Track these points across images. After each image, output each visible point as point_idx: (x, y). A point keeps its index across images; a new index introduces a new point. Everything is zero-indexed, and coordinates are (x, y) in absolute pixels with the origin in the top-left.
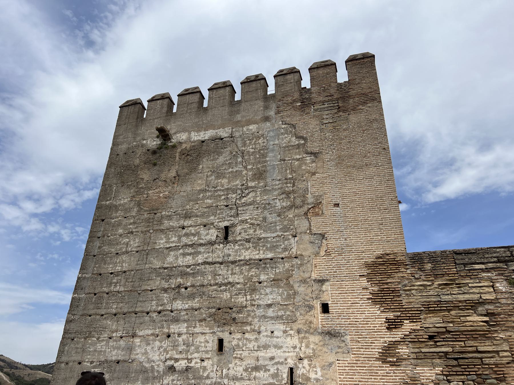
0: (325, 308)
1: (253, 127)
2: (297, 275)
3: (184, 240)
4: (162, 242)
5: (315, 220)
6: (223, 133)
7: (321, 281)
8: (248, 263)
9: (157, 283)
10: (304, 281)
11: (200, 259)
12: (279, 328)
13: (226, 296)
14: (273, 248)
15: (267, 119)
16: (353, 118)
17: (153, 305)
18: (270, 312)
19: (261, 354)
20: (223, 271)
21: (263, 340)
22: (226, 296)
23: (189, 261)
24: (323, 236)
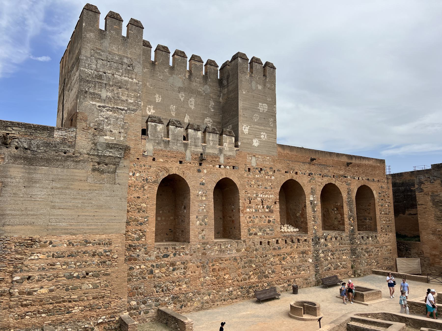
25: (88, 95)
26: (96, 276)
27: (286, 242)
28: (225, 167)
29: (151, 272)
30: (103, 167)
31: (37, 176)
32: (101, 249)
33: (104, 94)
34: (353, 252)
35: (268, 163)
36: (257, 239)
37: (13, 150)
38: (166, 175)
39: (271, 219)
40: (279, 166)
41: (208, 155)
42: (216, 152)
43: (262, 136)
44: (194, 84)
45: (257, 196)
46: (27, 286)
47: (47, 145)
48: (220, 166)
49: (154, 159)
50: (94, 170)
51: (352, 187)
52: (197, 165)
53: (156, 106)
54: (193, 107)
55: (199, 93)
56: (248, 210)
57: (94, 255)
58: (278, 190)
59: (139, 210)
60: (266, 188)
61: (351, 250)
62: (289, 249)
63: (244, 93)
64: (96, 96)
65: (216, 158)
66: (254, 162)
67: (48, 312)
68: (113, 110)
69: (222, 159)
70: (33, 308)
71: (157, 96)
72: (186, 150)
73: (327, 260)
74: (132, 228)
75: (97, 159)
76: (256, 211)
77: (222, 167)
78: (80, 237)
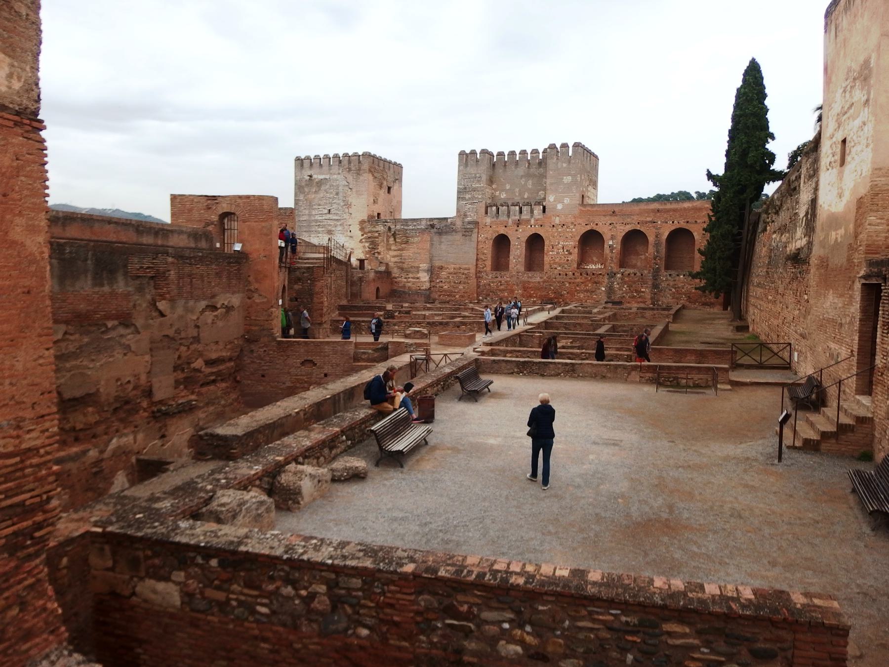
2: (345, 224)
3: (320, 212)
4: (314, 213)
6: (327, 177)
8: (335, 220)
9: (314, 224)
15: (339, 174)
16: (361, 178)
20: (329, 221)
23: (321, 218)
26: (464, 283)
27: (581, 274)
29: (489, 285)
30: (467, 233)
31: (443, 240)
32: (466, 272)
33: (468, 196)
34: (655, 286)
36: (556, 272)
37: (435, 230)
40: (580, 221)
41: (523, 220)
42: (528, 217)
43: (565, 201)
44: (532, 170)
45: (559, 243)
46: (441, 284)
51: (661, 231)
52: (516, 227)
53: (507, 191)
54: (530, 187)
55: (535, 176)
58: (578, 238)
59: (484, 254)
61: (653, 284)
64: (464, 199)
66: (557, 220)
67: (448, 295)
68: (471, 204)
74: (480, 263)
78: (458, 266)
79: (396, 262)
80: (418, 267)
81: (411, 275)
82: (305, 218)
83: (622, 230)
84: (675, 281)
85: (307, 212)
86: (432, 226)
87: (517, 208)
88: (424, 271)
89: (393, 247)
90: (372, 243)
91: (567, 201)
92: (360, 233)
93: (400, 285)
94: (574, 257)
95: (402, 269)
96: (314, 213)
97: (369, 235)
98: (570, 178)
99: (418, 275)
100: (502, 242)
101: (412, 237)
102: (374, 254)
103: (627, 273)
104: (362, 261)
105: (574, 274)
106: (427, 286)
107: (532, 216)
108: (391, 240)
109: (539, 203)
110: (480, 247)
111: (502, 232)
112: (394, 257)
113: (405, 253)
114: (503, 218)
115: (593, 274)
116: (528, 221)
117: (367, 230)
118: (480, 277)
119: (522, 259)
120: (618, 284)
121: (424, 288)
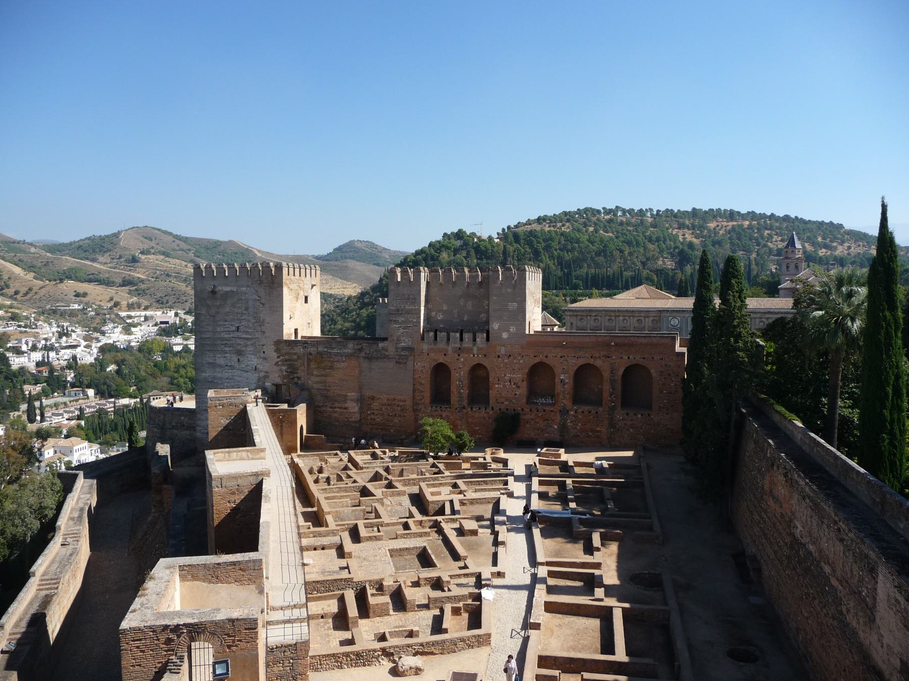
0: (264, 352)
1: (244, 289)
2: (257, 343)
5: (263, 327)
6: (234, 289)
7: (263, 345)
8: (244, 338)
9: (219, 342)
10: (259, 345)
11: (231, 336)
12: (253, 356)
13: (239, 347)
14: (251, 335)
15: (248, 286)
17: (219, 348)
18: (251, 353)
19: (249, 363)
21: (249, 359)
22: (239, 347)
23: (227, 336)
24: (264, 332)
25: (393, 322)
26: (400, 416)
27: (531, 410)
28: (478, 355)
33: (401, 319)
34: (612, 425)
35: (517, 350)
38: (436, 363)
39: (517, 393)
43: (511, 330)
45: (505, 375)
46: (373, 416)
47: (376, 351)
48: (474, 355)
49: (428, 354)
50: (397, 362)
52: (457, 355)
54: (470, 308)
56: (497, 386)
57: (398, 406)
58: (526, 371)
59: (421, 384)
60: (514, 369)
62: (532, 417)
63: (495, 298)
64: (396, 322)
65: (471, 350)
66: (503, 351)
69: (475, 350)
70: (375, 427)
71: (444, 305)
72: (448, 346)
73: (576, 428)
75: (398, 357)
76: (503, 386)
77: (476, 356)
79: (319, 389)
80: (346, 396)
81: (337, 405)
82: (208, 335)
83: (574, 363)
84: (632, 420)
85: (210, 328)
86: (361, 350)
87: (458, 335)
88: (352, 400)
89: (315, 373)
90: (290, 366)
91: (512, 329)
92: (275, 355)
93: (325, 415)
94: (523, 391)
95: (327, 397)
96: (219, 329)
97: (287, 357)
98: (515, 304)
99: (346, 405)
100: (441, 372)
101: (338, 361)
102: (293, 379)
103: (580, 410)
104: (277, 386)
105: (523, 410)
106: (357, 417)
107: (474, 345)
108: (313, 365)
109: (482, 331)
110: (417, 376)
111: (441, 360)
112: (317, 383)
113: (329, 379)
114: (442, 345)
115: (544, 411)
116: (469, 350)
117: (284, 352)
118: (417, 410)
119: (465, 392)
120: (571, 422)
121: (353, 419)
